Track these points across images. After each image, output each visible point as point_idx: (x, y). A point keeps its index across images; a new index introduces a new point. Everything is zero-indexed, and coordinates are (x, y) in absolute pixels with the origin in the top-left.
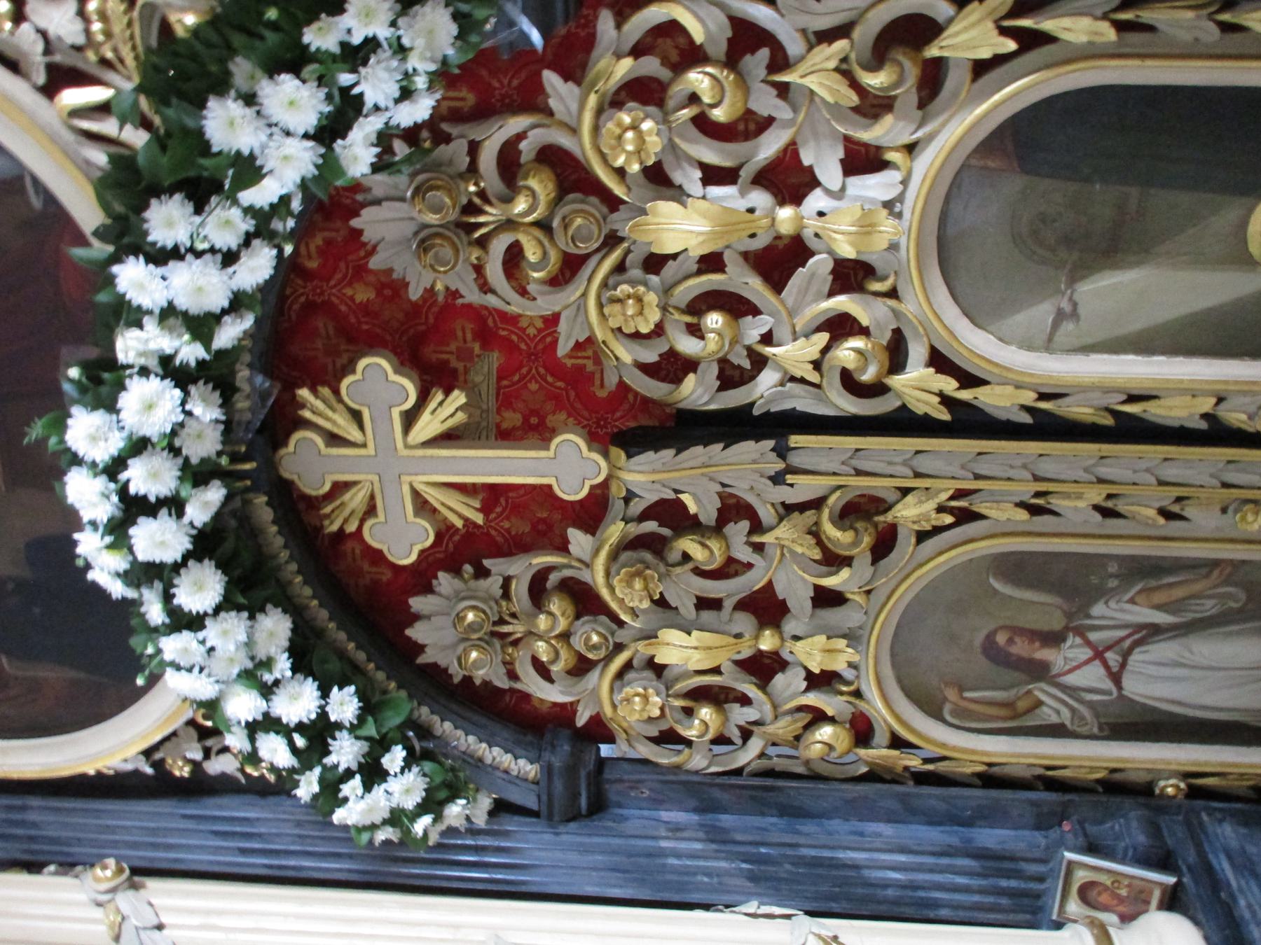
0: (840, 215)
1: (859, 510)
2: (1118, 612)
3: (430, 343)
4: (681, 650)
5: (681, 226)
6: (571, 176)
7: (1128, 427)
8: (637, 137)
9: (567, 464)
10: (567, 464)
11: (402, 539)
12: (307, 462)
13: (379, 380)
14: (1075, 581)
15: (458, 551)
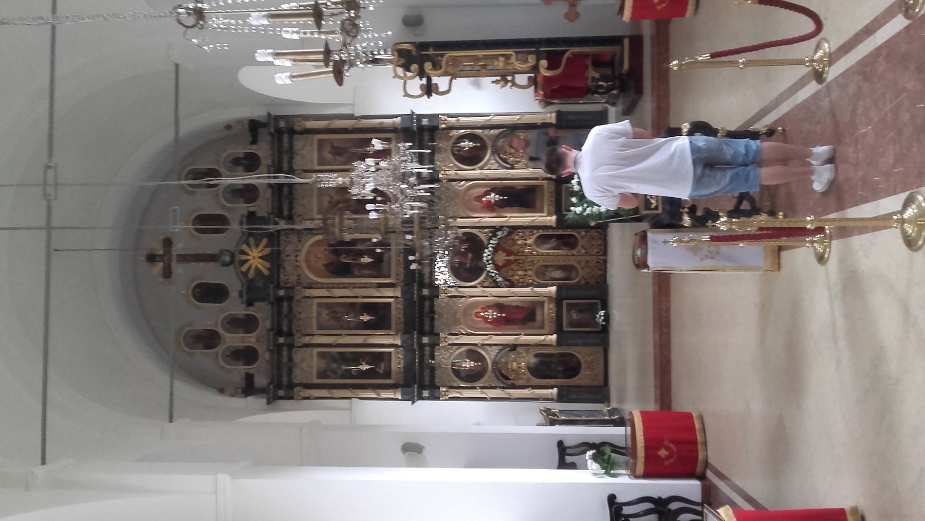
0: (529, 242)
1: (532, 262)
2: (550, 269)
3: (504, 250)
4: (520, 273)
5: (519, 242)
6: (513, 240)
7: (548, 254)
8: (517, 237)
9: (512, 258)
10: (512, 258)
11: (501, 264)
12: (495, 259)
13: (500, 252)
14: (546, 267)
15: (505, 266)
